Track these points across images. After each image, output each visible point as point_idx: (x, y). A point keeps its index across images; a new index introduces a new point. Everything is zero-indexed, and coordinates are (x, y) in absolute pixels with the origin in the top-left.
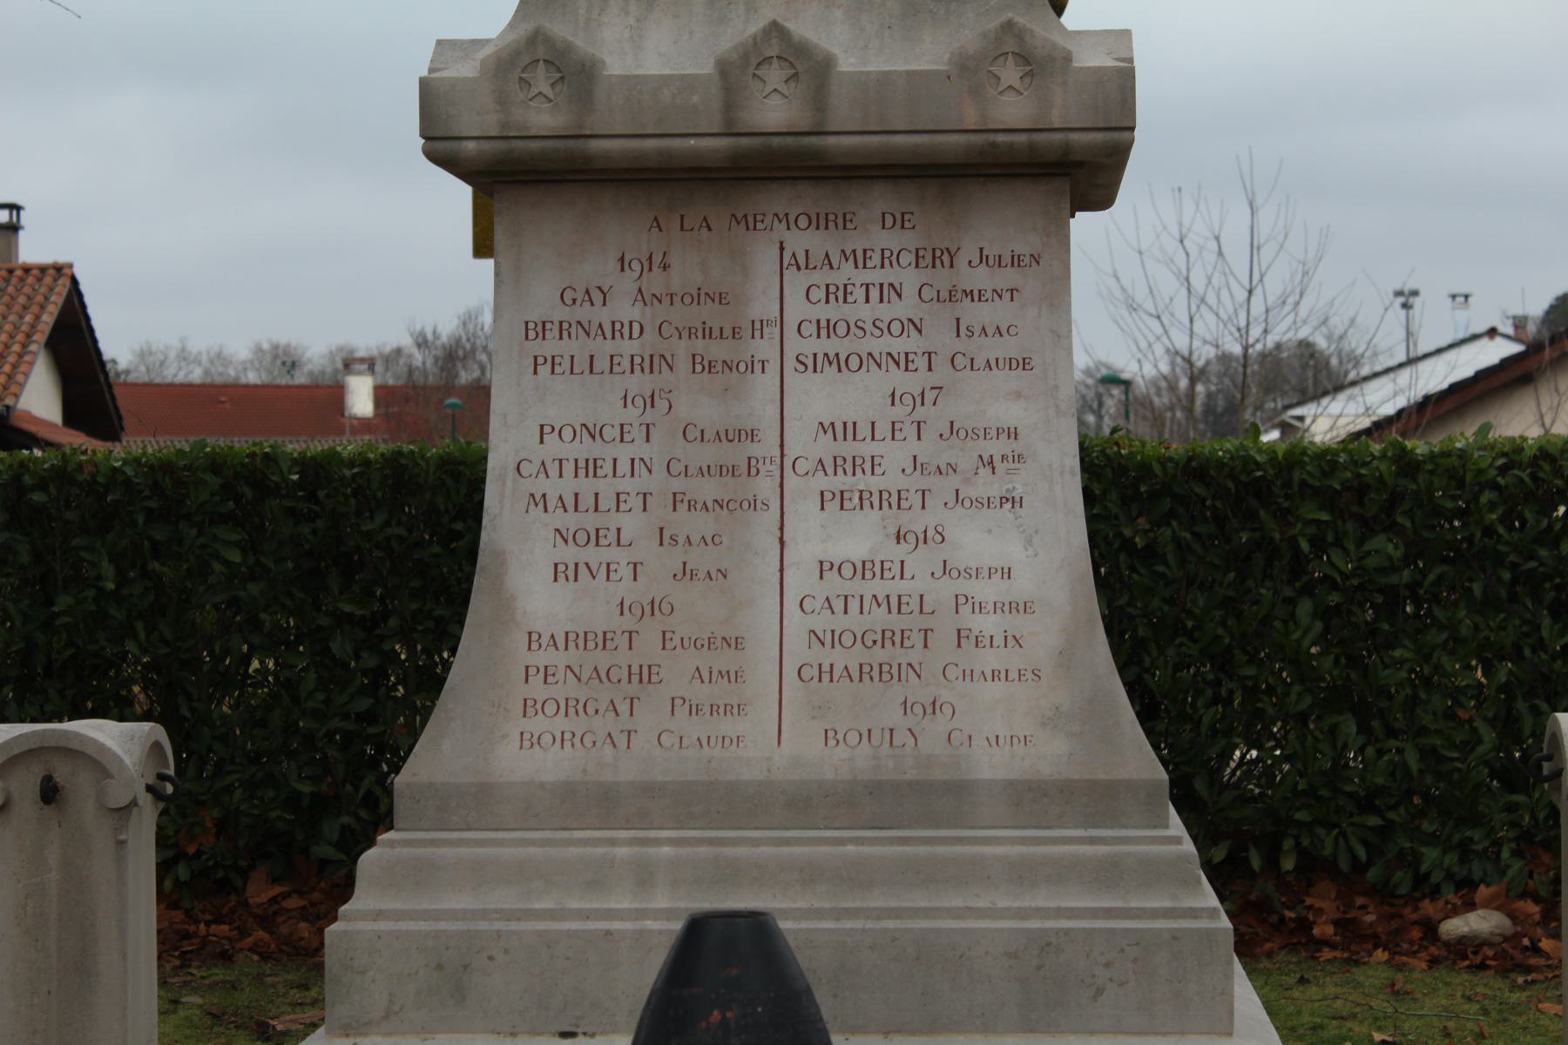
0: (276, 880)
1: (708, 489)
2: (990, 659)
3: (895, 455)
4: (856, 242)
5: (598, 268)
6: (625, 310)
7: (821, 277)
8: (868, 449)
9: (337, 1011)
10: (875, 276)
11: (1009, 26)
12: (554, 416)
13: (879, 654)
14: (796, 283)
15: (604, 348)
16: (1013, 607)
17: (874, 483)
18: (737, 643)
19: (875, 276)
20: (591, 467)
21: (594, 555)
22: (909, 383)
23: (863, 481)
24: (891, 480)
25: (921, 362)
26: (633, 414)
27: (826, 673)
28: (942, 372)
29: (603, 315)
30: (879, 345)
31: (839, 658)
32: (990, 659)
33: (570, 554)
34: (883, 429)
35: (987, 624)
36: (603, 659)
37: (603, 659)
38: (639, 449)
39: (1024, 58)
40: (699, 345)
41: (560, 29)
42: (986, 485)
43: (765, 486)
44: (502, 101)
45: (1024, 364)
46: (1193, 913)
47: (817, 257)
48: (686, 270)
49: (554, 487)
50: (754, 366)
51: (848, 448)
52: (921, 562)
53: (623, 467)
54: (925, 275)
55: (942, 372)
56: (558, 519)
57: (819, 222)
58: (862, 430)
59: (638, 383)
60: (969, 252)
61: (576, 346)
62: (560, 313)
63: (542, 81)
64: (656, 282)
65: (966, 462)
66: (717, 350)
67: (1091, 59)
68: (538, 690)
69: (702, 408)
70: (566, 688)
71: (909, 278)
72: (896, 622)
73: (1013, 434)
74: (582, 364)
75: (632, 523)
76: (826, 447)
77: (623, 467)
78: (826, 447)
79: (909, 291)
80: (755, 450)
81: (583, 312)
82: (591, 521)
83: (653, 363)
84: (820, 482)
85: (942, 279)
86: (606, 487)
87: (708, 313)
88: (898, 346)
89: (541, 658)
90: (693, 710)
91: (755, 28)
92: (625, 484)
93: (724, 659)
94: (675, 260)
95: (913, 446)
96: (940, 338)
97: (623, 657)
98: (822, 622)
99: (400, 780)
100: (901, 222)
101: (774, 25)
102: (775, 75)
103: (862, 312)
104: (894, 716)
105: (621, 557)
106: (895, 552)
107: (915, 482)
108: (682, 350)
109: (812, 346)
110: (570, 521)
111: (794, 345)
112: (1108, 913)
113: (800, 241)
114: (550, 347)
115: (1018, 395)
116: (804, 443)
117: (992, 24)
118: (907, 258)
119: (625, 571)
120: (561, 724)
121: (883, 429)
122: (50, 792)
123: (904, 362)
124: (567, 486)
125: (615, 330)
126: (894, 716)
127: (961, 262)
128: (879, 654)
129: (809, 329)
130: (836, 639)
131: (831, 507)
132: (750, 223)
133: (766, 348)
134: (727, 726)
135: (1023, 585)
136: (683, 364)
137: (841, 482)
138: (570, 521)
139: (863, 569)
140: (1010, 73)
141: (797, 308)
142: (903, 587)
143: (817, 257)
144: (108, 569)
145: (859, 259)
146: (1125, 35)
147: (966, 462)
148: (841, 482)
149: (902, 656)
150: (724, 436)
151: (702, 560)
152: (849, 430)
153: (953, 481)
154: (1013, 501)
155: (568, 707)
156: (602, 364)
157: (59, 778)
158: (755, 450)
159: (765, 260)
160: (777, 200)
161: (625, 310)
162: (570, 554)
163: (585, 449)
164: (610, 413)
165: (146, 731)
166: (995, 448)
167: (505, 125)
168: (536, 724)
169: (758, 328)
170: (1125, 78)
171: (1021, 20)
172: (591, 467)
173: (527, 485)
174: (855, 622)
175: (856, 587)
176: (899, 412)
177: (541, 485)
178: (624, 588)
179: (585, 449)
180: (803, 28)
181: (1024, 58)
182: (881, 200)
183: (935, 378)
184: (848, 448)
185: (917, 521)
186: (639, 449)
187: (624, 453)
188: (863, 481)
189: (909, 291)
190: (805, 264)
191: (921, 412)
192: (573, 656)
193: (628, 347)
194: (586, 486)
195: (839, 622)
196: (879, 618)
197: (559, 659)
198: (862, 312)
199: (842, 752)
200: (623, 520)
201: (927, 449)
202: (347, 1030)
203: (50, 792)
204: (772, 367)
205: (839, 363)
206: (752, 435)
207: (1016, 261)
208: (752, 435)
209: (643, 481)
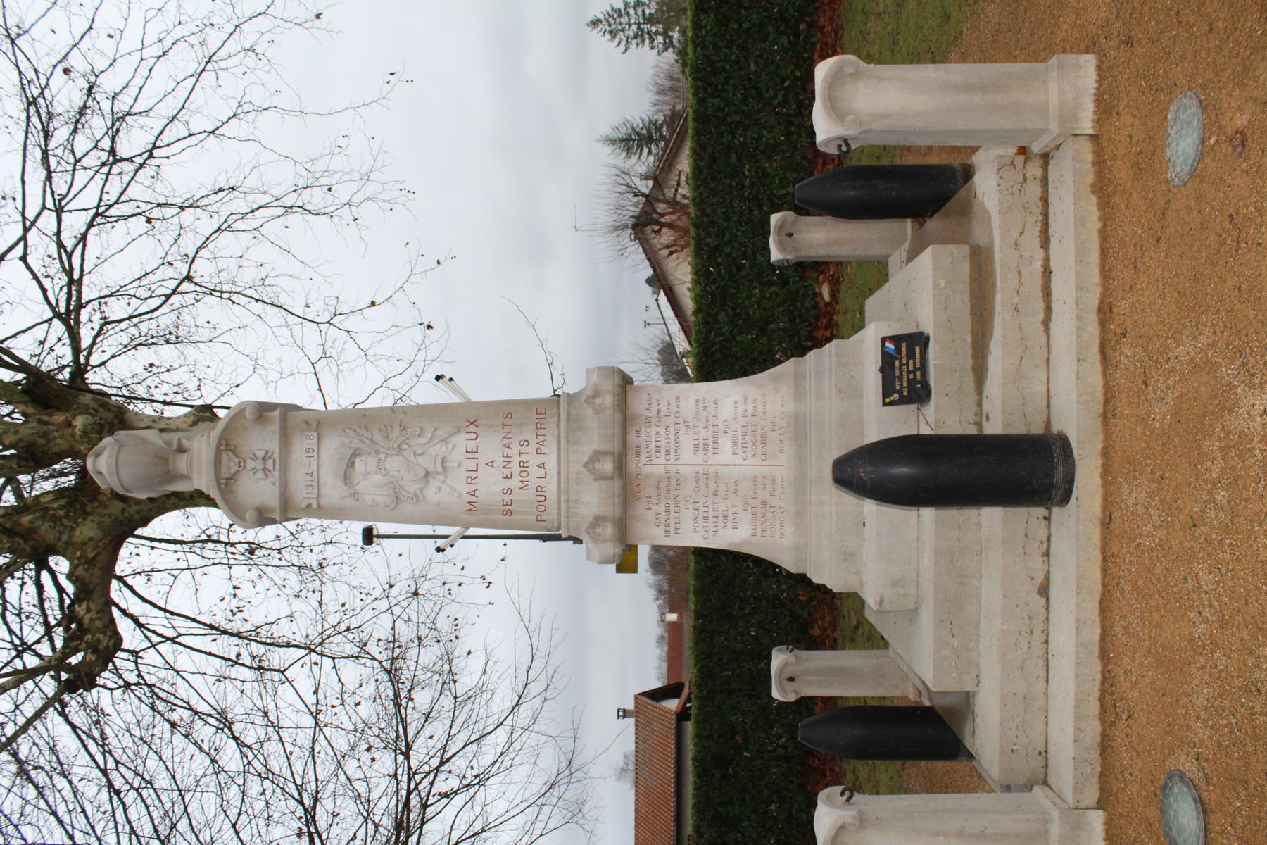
0: (813, 627)
1: (712, 486)
2: (760, 408)
3: (703, 434)
4: (644, 445)
5: (650, 516)
6: (662, 508)
7: (653, 454)
8: (701, 441)
9: (856, 589)
10: (653, 438)
11: (585, 401)
12: (691, 528)
13: (759, 438)
14: (655, 461)
15: (672, 515)
16: (745, 401)
17: (711, 440)
18: (755, 478)
19: (653, 438)
20: (706, 518)
21: (730, 517)
22: (683, 430)
23: (710, 443)
24: (710, 435)
25: (677, 426)
26: (691, 507)
27: (764, 453)
28: (679, 420)
29: (664, 514)
30: (672, 437)
31: (759, 449)
32: (760, 408)
33: (730, 524)
34: (696, 437)
35: (750, 408)
36: (760, 515)
37: (760, 515)
38: (701, 505)
39: (594, 397)
40: (672, 488)
41: (585, 526)
42: (712, 408)
43: (711, 469)
44: (604, 541)
45: (678, 398)
46: (830, 352)
47: (648, 455)
48: (650, 491)
49: (711, 529)
50: (678, 472)
51: (701, 447)
52: (733, 427)
53: (706, 509)
54: (653, 425)
55: (679, 420)
56: (720, 528)
57: (638, 454)
58: (696, 442)
59: (682, 505)
60: (647, 413)
61: (672, 522)
62: (663, 527)
63: (599, 530)
64: (654, 500)
65: (705, 414)
66: (673, 483)
67: (595, 378)
68: (768, 533)
69: (688, 488)
70: (767, 526)
71: (654, 430)
72: (749, 433)
73: (697, 401)
74: (677, 521)
75: (722, 506)
76: (701, 453)
77: (706, 509)
78: (701, 453)
79: (657, 429)
80: (701, 472)
81: (662, 520)
82: (721, 519)
83: (677, 501)
84: (710, 454)
85: (654, 420)
86: (711, 514)
87: (663, 485)
88: (672, 433)
89: (759, 531)
90: (774, 490)
91: (584, 471)
92: (711, 509)
93: (760, 482)
94: (648, 494)
95: (700, 429)
96: (671, 421)
97: (759, 509)
98: (749, 454)
99: (793, 571)
100: (638, 431)
101: (585, 465)
102: (598, 466)
103: (663, 442)
104: (776, 434)
105: (731, 510)
106: (730, 433)
107: (711, 429)
108: (673, 493)
109: (672, 457)
110: (721, 524)
111: (672, 461)
112: (830, 374)
113: (643, 460)
114: (672, 529)
115: (686, 400)
116: (699, 459)
117: (585, 405)
118: (648, 430)
119: (735, 509)
120: (777, 527)
121: (696, 437)
122: (791, 679)
123: (677, 431)
124: (711, 525)
125: (667, 511)
126: (776, 434)
127: (649, 415)
128: (759, 438)
129: (668, 457)
130: (754, 450)
131: (717, 451)
132: (638, 474)
133: (673, 469)
134: (778, 480)
135: (739, 398)
136: (677, 492)
137: (710, 449)
138: (721, 524)
139: (735, 443)
140: (598, 401)
141: (662, 461)
142: (740, 432)
143: (648, 455)
144: (726, 673)
145: (648, 443)
146: (587, 370)
147: (705, 414)
148: (710, 449)
149: (759, 431)
150: (697, 481)
151: (732, 487)
152: (696, 446)
153: (710, 417)
154: (716, 402)
155: (773, 525)
156: (677, 515)
157: (788, 676)
158: (701, 472)
159: (648, 469)
160: (631, 466)
161: (662, 508)
162: (730, 524)
163: (700, 520)
164: (691, 513)
165: (774, 652)
166: (701, 405)
167: (611, 541)
168: (778, 535)
169: (667, 472)
170: (600, 369)
171: (584, 398)
172: (706, 518)
173: (711, 536)
174: (749, 445)
175: (740, 444)
176: (691, 432)
177: (711, 532)
178: (739, 509)
179: (700, 520)
180: (585, 459)
181: (594, 397)
182: (631, 437)
183: (682, 423)
184: (701, 447)
185: (721, 428)
186: (701, 505)
187: (702, 509)
188: (710, 443)
189: (657, 429)
190: (650, 459)
191: (691, 426)
192: (759, 524)
193: (672, 508)
194: (711, 520)
195: (749, 449)
196: (748, 438)
197: (759, 528)
198: (663, 442)
199: (786, 448)
200: (720, 510)
201: (701, 424)
202: (862, 586)
203: (791, 679)
204: (678, 467)
205: (677, 449)
206: (697, 473)
207: (649, 400)
208: (697, 473)
209: (709, 503)
